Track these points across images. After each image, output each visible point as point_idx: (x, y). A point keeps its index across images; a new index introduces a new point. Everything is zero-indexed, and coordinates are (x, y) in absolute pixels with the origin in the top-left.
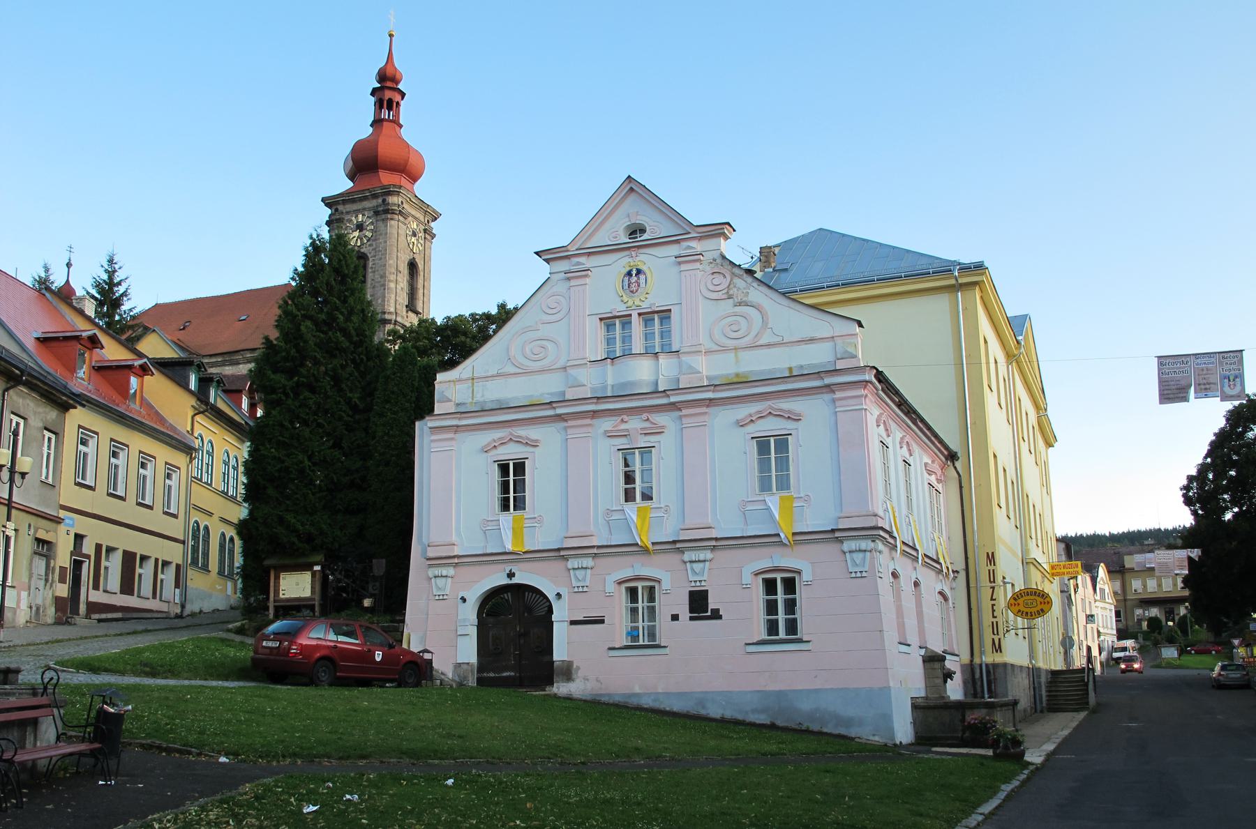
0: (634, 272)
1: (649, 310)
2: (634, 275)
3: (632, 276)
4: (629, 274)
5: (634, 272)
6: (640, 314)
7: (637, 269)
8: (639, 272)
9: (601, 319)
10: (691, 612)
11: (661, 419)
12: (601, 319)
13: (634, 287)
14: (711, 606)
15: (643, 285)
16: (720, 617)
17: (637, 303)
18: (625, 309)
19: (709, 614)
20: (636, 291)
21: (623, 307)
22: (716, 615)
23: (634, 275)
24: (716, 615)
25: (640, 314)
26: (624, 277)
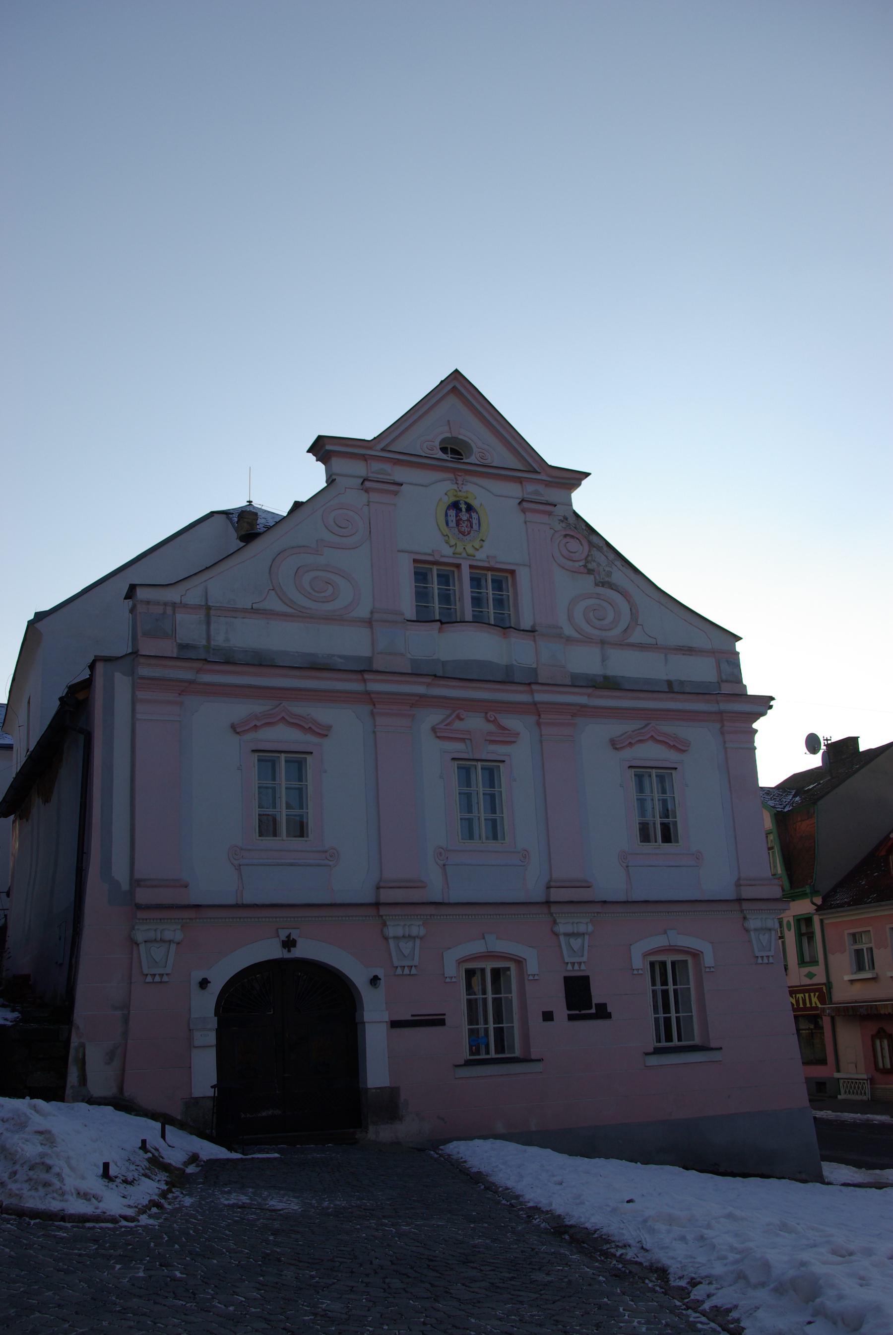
0: (463, 507)
1: (486, 565)
2: (464, 510)
3: (461, 510)
4: (455, 505)
5: (463, 507)
6: (471, 567)
7: (466, 503)
8: (470, 508)
9: (415, 561)
10: (569, 1008)
11: (512, 722)
12: (415, 561)
13: (464, 527)
14: (596, 1000)
15: (475, 527)
16: (608, 1016)
17: (470, 550)
18: (451, 554)
19: (593, 1011)
20: (469, 533)
21: (448, 551)
22: (603, 1013)
23: (464, 510)
24: (603, 1013)
25: (471, 567)
26: (448, 508)
